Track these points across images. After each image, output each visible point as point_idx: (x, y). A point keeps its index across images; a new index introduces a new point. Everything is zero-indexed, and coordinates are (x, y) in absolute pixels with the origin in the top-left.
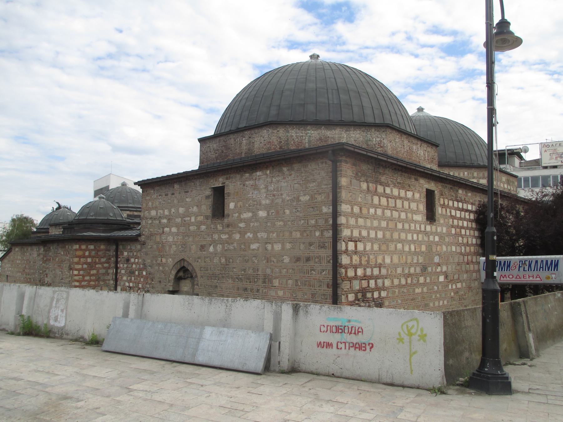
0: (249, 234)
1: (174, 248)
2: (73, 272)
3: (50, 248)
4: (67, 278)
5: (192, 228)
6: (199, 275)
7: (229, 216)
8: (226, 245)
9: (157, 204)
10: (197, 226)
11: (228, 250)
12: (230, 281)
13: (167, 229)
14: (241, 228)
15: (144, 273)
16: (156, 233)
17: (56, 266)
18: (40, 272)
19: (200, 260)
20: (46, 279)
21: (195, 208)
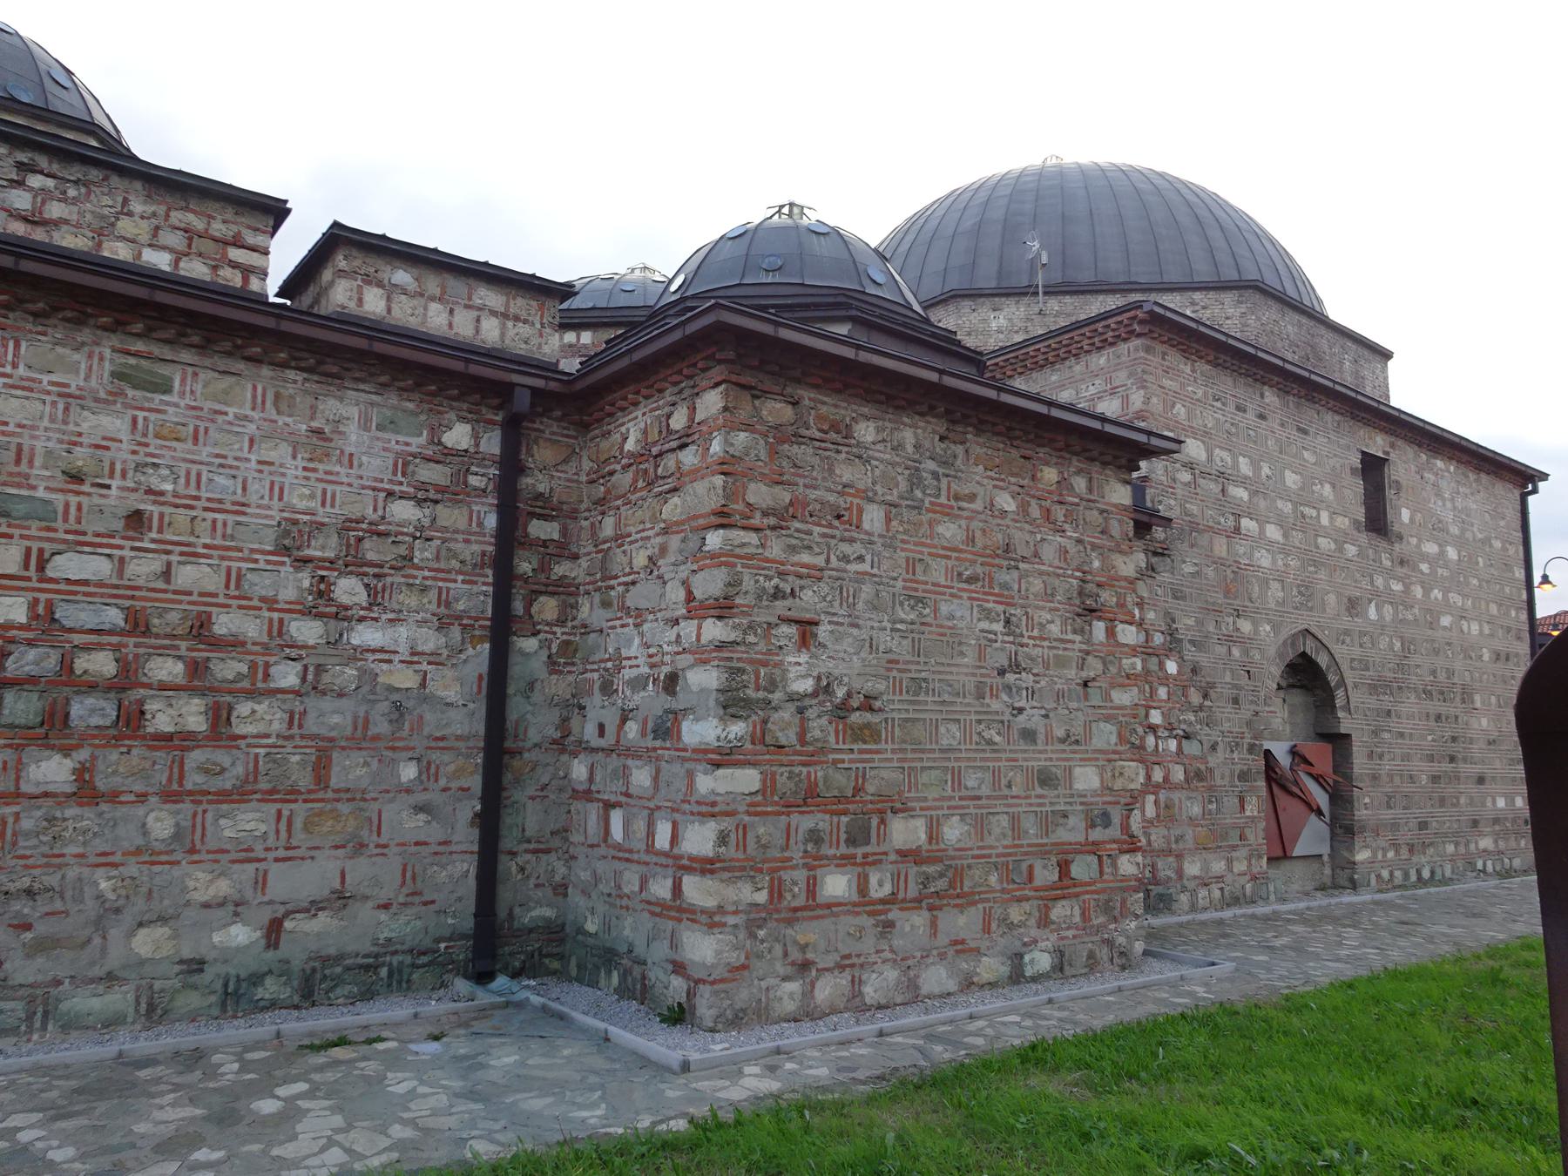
0: (1436, 591)
1: (1275, 591)
2: (1111, 632)
4: (1061, 663)
5: (1323, 542)
6: (1349, 681)
8: (1401, 607)
9: (1209, 425)
10: (1335, 541)
12: (1413, 699)
14: (1422, 573)
15: (1172, 667)
16: (1211, 524)
17: (938, 572)
19: (1348, 640)
21: (1328, 488)
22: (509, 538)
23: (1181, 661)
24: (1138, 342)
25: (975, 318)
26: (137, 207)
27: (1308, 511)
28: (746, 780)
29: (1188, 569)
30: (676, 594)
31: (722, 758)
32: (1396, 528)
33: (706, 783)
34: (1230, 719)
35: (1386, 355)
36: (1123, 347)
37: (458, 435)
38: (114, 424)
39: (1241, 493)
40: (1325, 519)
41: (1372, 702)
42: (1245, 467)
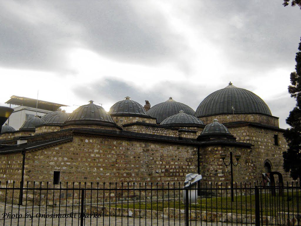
1: (264, 155)
2: (248, 164)
3: (228, 149)
5: (270, 148)
7: (279, 145)
11: (280, 157)
13: (260, 147)
18: (150, 166)
20: (226, 169)
21: (270, 140)
22: (199, 158)
23: (253, 164)
24: (248, 127)
25: (225, 117)
26: (171, 131)
27: (268, 144)
28: (223, 179)
29: (254, 153)
30: (216, 163)
31: (222, 177)
32: (279, 144)
33: (221, 179)
34: (258, 171)
35: (278, 118)
36: (246, 127)
37: (195, 149)
38: (177, 152)
39: (259, 143)
40: (270, 145)
41: (276, 168)
42: (260, 140)
